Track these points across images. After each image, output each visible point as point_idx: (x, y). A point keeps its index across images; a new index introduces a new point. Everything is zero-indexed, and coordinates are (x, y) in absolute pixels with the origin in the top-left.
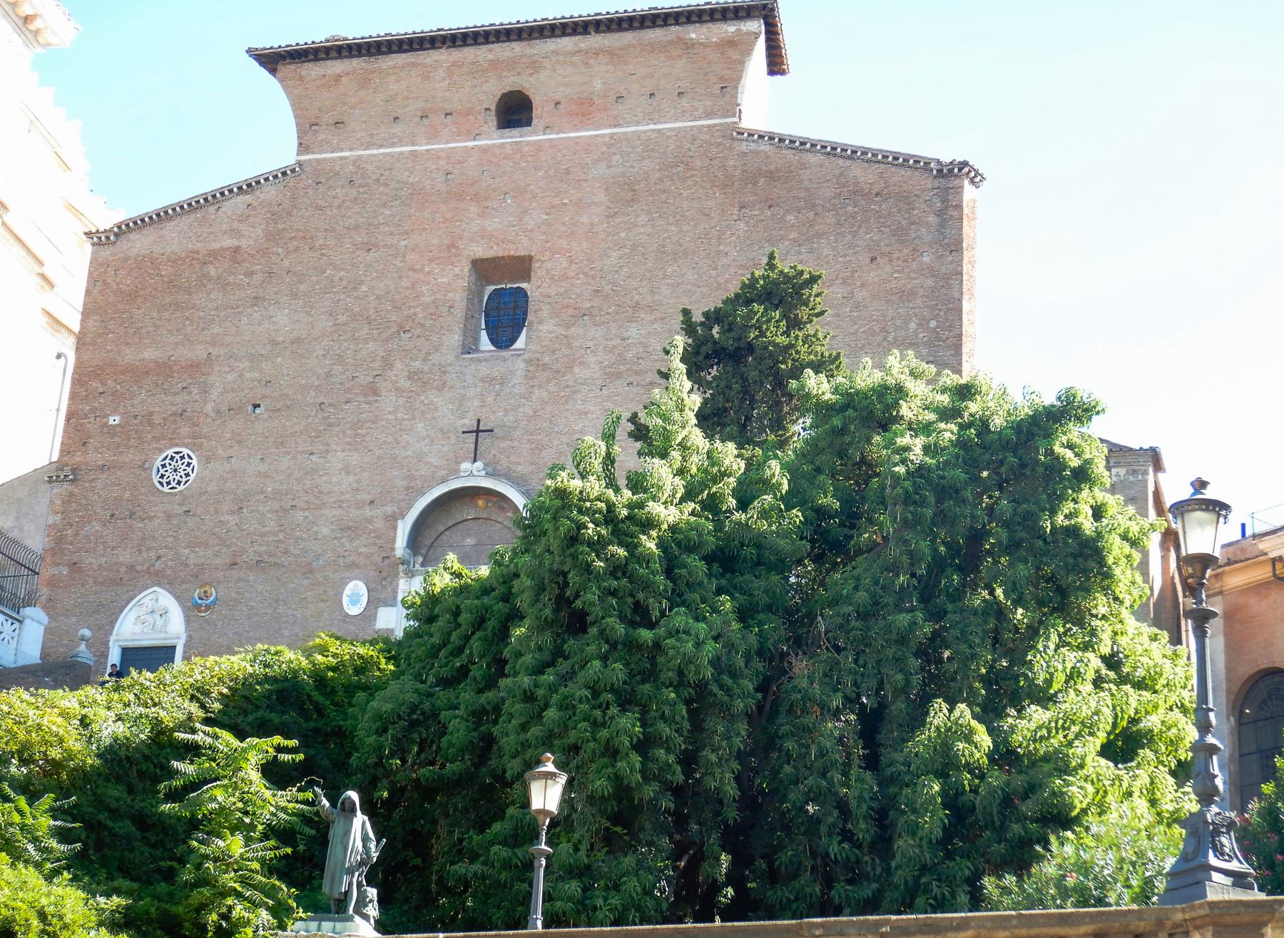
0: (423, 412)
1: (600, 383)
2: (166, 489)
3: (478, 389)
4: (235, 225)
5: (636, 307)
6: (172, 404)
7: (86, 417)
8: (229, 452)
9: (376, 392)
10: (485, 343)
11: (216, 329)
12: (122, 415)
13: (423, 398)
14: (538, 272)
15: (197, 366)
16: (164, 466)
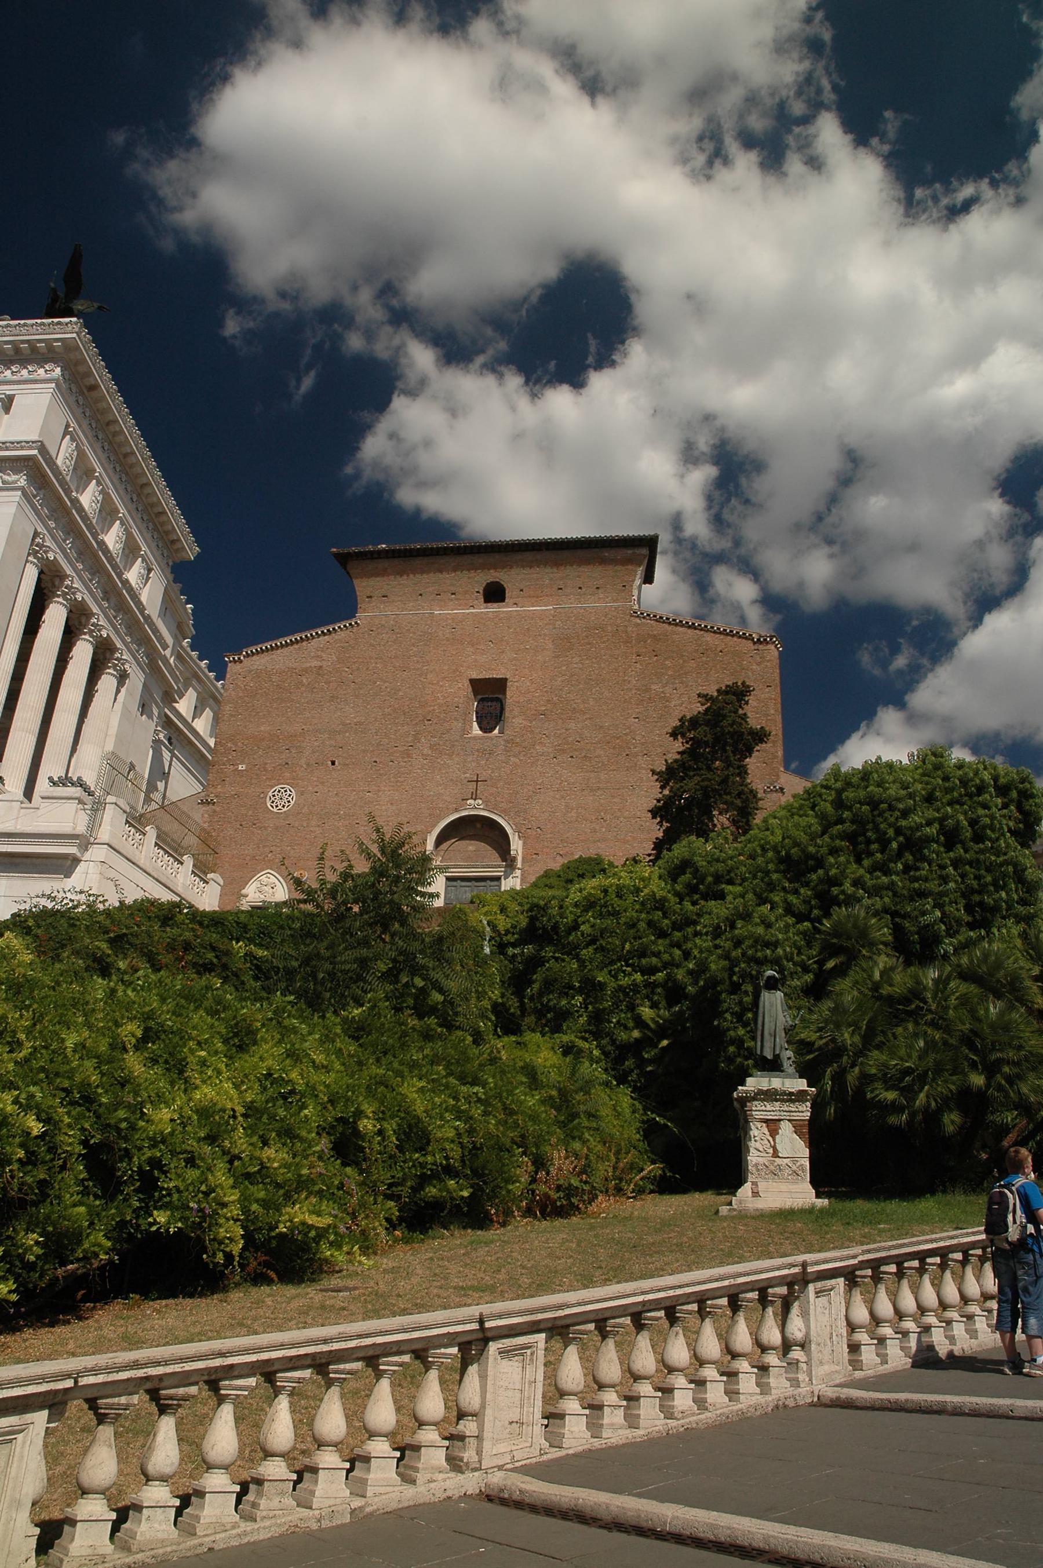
2: (275, 810)
4: (319, 653)
7: (224, 764)
8: (316, 789)
9: (409, 756)
10: (476, 731)
11: (308, 715)
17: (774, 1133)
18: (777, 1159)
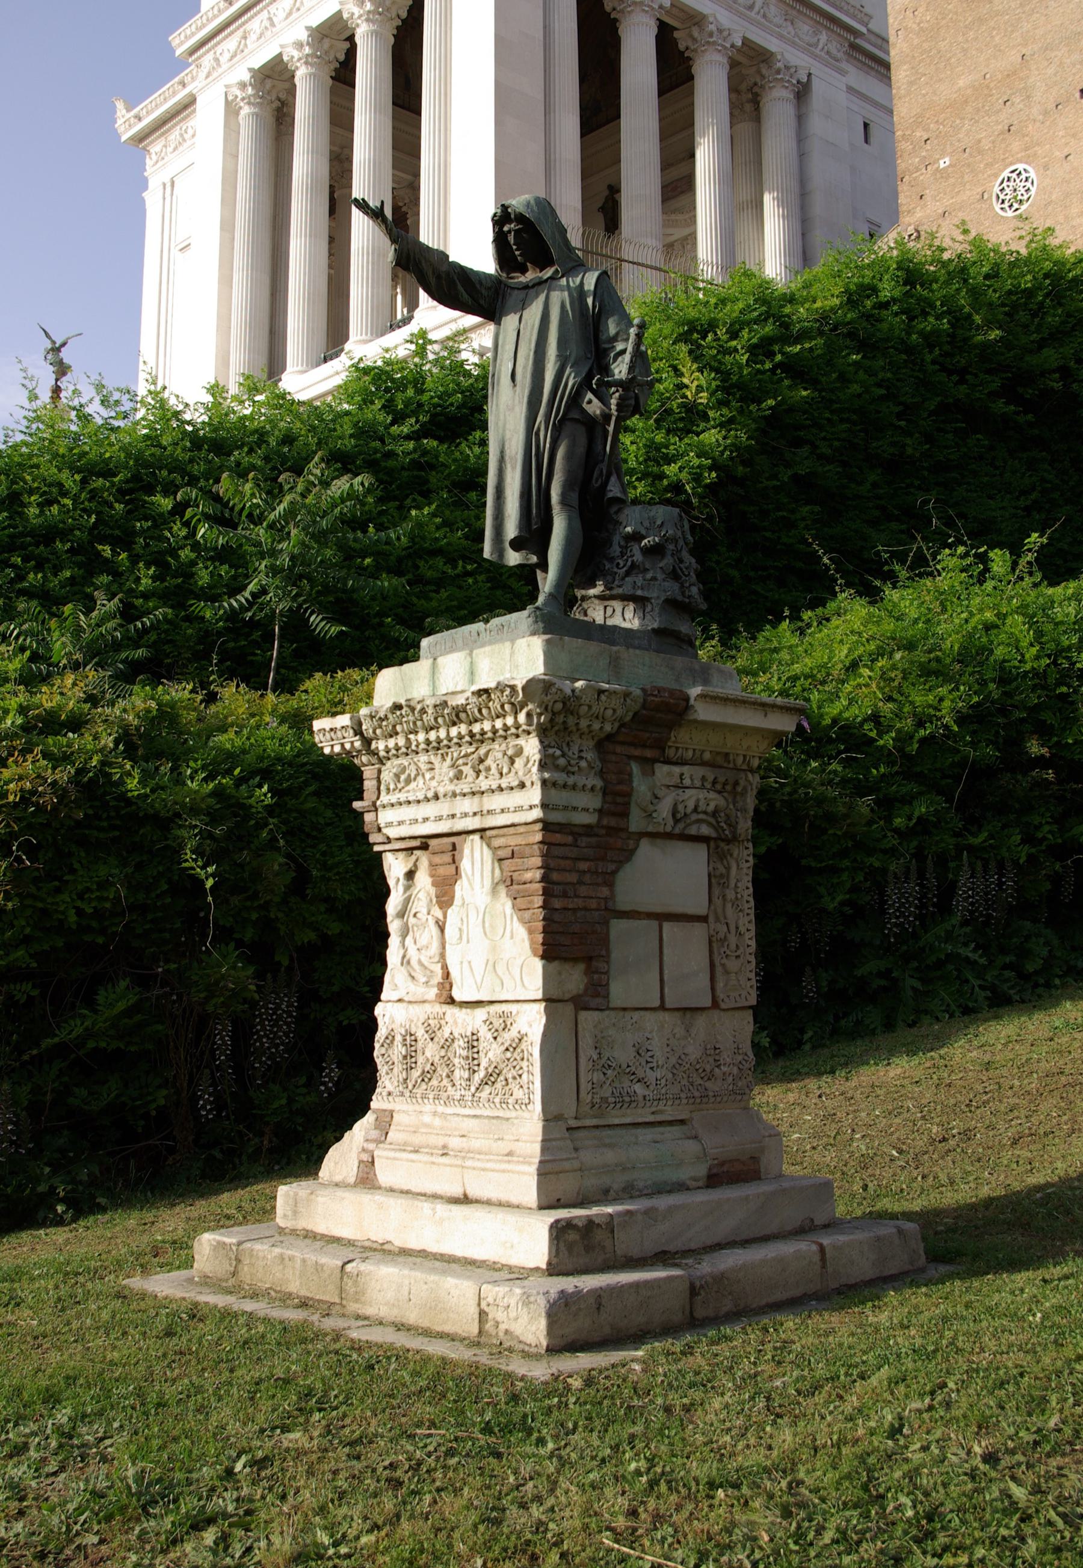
6: (997, 123)
12: (951, 154)
15: (1015, 73)
16: (1002, 190)
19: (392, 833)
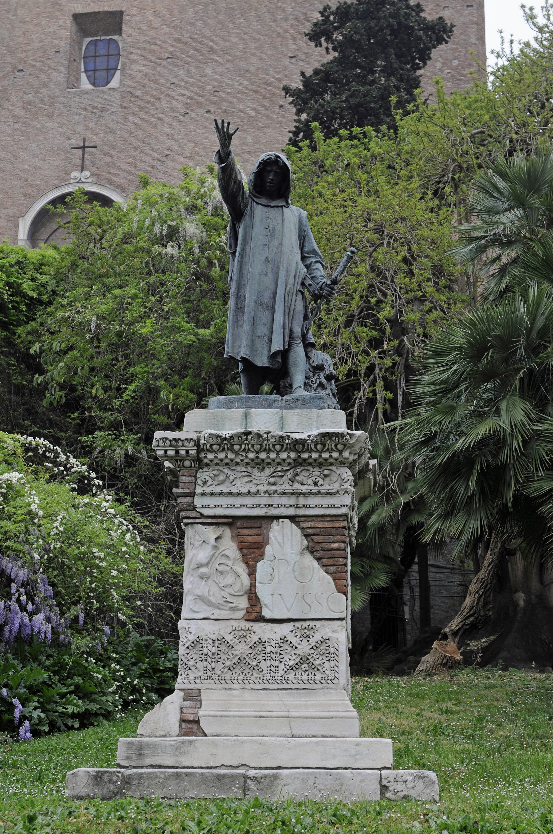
0: (37, 135)
1: (183, 111)
3: (82, 116)
5: (211, 51)
10: (85, 84)
13: (35, 123)
14: (128, 26)
17: (252, 553)
18: (258, 627)
19: (206, 512)
